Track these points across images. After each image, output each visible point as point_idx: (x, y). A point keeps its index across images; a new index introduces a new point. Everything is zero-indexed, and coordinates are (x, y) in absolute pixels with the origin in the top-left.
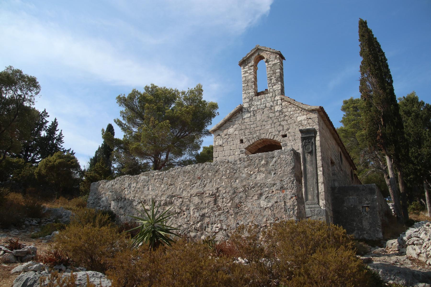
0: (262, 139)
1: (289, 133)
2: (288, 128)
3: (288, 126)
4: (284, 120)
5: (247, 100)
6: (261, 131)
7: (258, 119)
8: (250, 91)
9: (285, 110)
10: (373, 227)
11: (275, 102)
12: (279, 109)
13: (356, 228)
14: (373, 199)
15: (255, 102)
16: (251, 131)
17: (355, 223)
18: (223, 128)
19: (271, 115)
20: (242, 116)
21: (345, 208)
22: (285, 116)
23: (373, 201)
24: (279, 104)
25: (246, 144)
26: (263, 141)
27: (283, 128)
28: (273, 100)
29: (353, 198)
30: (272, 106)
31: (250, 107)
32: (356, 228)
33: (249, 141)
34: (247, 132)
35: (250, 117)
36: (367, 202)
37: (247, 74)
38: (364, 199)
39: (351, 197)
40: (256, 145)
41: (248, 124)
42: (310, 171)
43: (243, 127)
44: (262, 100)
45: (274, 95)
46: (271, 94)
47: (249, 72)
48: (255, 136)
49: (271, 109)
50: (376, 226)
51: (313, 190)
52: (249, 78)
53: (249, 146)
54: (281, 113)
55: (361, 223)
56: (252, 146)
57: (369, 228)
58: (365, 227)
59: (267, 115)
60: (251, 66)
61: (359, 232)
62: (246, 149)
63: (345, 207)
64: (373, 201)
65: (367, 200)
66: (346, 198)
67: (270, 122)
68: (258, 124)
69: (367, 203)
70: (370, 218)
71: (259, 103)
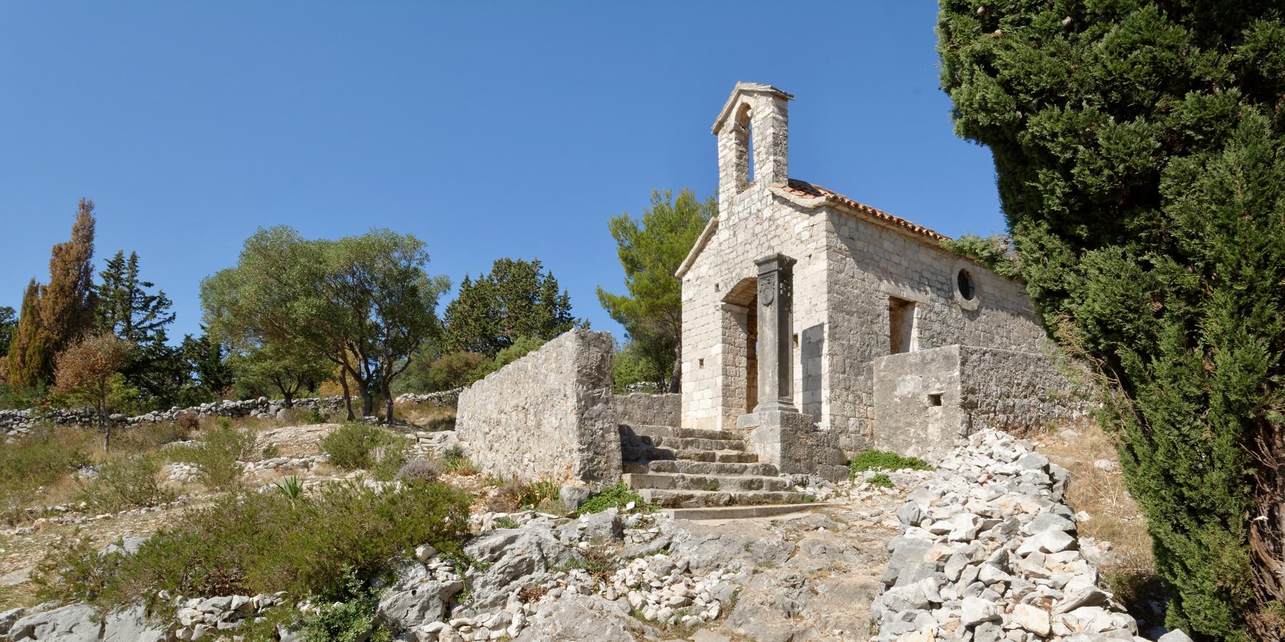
0: (745, 280)
4: (775, 236)
5: (726, 205)
6: (744, 265)
7: (739, 241)
8: (729, 185)
9: (777, 215)
11: (764, 201)
12: (769, 215)
13: (914, 441)
15: (736, 208)
16: (730, 266)
17: (913, 430)
18: (693, 267)
19: (758, 228)
20: (718, 238)
21: (897, 400)
22: (777, 227)
23: (950, 383)
24: (769, 203)
25: (723, 294)
26: (752, 282)
28: (761, 196)
29: (912, 379)
30: (759, 211)
31: (729, 218)
32: (914, 441)
33: (726, 286)
34: (723, 269)
35: (729, 239)
36: (938, 385)
37: (726, 151)
39: (909, 377)
40: (742, 292)
41: (726, 252)
43: (719, 260)
44: (746, 201)
45: (763, 187)
46: (759, 184)
47: (728, 144)
48: (734, 275)
49: (758, 217)
51: (773, 376)
52: (728, 158)
53: (728, 295)
54: (771, 222)
55: (925, 429)
56: (734, 295)
58: (930, 437)
59: (751, 231)
60: (731, 132)
61: (920, 448)
62: (722, 301)
63: (897, 397)
64: (950, 383)
66: (900, 379)
67: (756, 243)
68: (740, 250)
70: (942, 418)
71: (740, 208)
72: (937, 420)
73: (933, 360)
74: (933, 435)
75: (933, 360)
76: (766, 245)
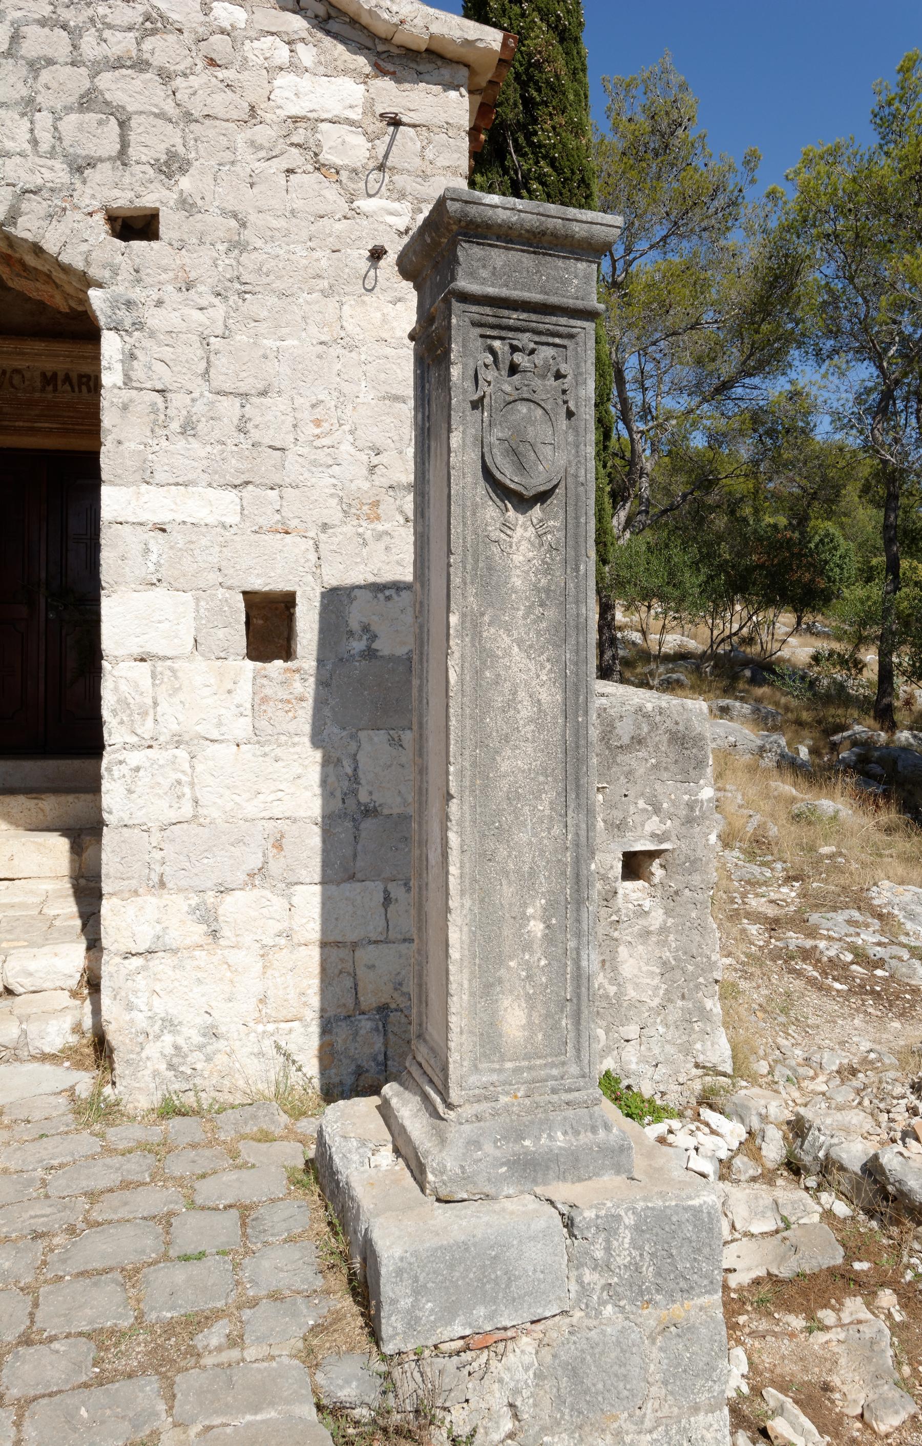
1: (186, 205)
2: (172, 156)
3: (172, 137)
4: (141, 65)
10: (683, 997)
14: (691, 806)
23: (689, 821)
27: (124, 145)
36: (653, 824)
38: (641, 804)
42: (526, 711)
50: (698, 987)
57: (656, 1001)
58: (632, 993)
64: (689, 821)
65: (657, 810)
69: (653, 835)
70: (664, 930)
72: (646, 934)
73: (638, 741)
74: (637, 986)
75: (638, 741)
76: (79, 79)
